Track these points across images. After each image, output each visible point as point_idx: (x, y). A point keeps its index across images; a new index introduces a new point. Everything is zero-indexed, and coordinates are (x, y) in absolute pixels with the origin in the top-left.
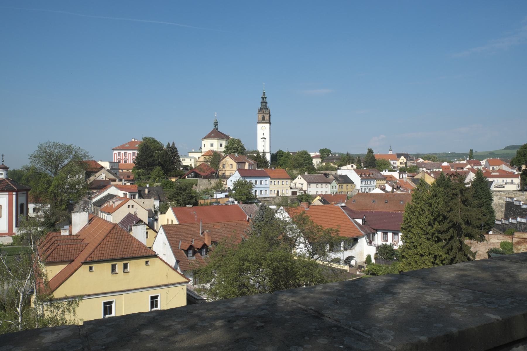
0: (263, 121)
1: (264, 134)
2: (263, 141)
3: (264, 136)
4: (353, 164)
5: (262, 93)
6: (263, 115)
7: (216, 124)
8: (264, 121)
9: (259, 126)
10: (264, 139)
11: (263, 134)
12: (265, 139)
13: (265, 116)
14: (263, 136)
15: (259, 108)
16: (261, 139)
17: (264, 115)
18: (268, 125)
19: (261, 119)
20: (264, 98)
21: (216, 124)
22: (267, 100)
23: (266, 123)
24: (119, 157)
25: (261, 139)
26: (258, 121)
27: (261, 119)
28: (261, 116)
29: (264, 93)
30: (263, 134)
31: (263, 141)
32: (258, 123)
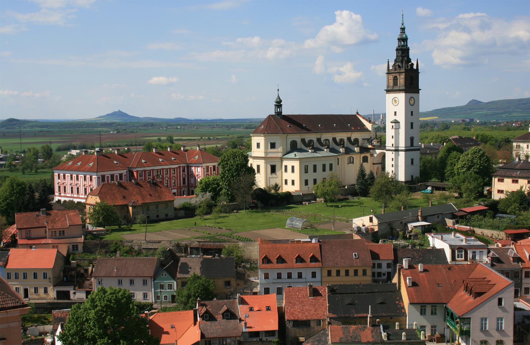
2: (393, 126)
3: (397, 118)
4: (371, 216)
5: (399, 31)
6: (394, 75)
7: (279, 104)
9: (390, 96)
10: (393, 124)
13: (398, 76)
15: (392, 64)
16: (392, 122)
17: (397, 75)
18: (401, 97)
19: (391, 82)
20: (403, 40)
21: (279, 104)
22: (409, 45)
23: (399, 91)
24: (59, 181)
26: (388, 86)
27: (391, 84)
28: (391, 77)
29: (403, 29)
31: (393, 126)
32: (388, 91)
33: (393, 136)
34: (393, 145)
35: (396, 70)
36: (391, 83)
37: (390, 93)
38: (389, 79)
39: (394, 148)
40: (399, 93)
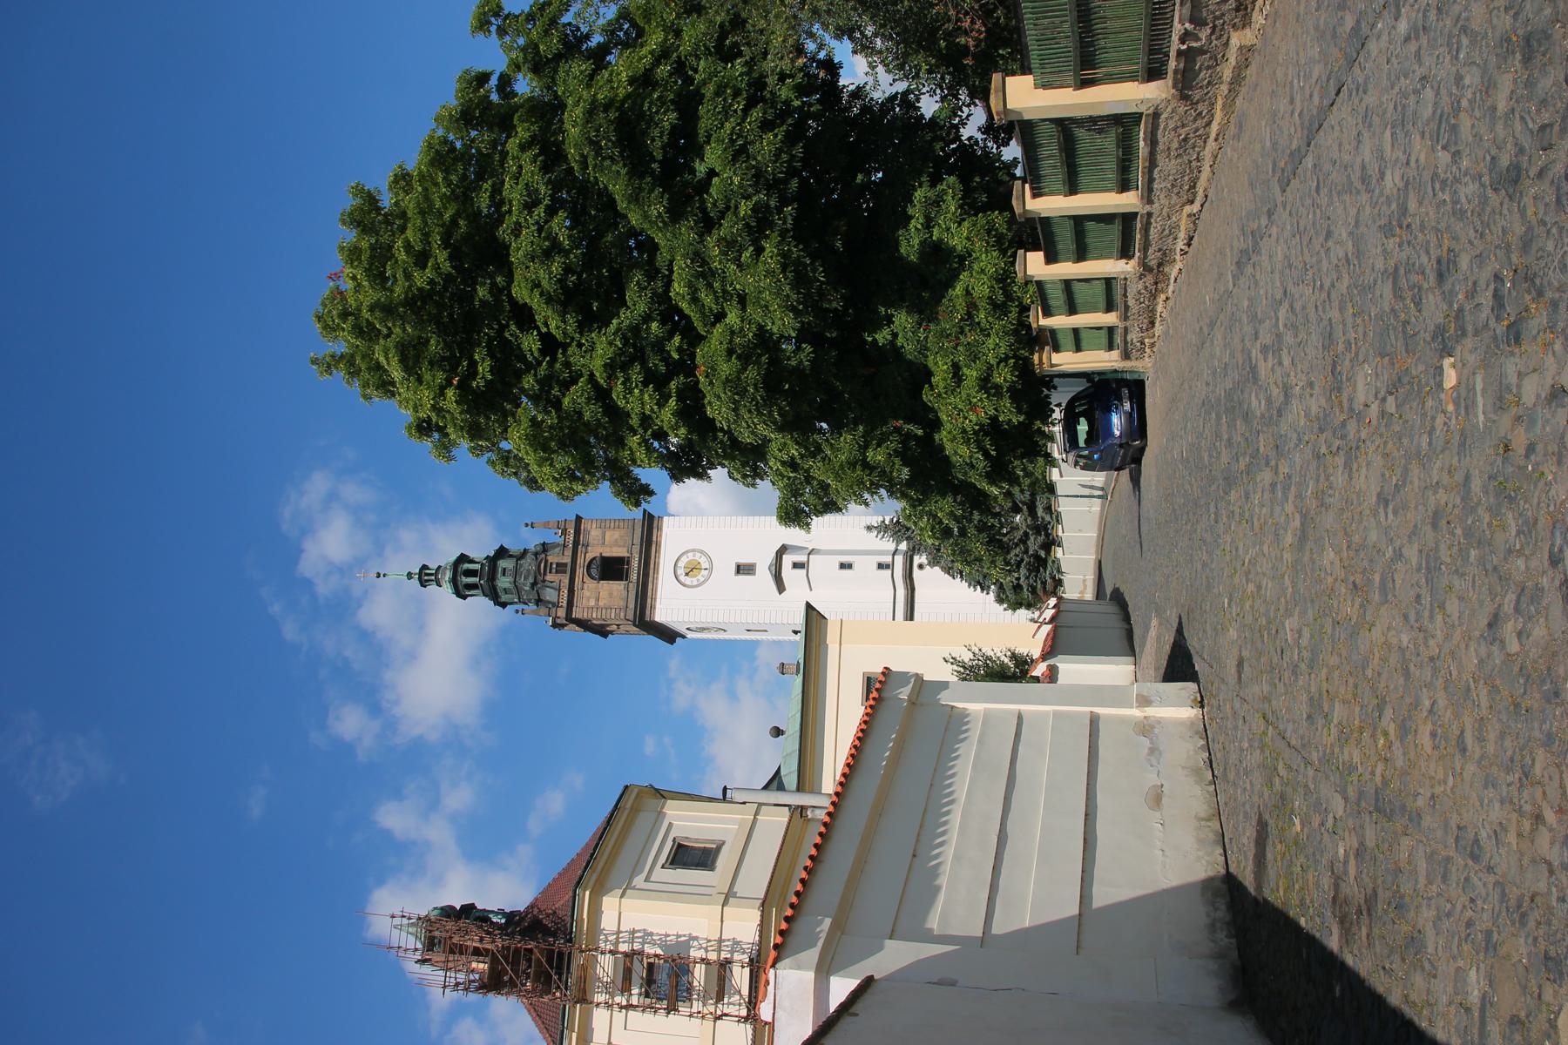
0: (634, 577)
1: (743, 560)
2: (796, 565)
3: (764, 562)
6: (580, 571)
8: (635, 564)
10: (788, 560)
11: (742, 569)
12: (783, 550)
14: (764, 575)
16: (781, 587)
17: (580, 560)
25: (781, 587)
27: (616, 587)
30: (742, 569)
31: (796, 565)
33: (843, 566)
34: (881, 566)
35: (565, 565)
36: (611, 595)
37: (654, 599)
38: (592, 603)
39: (899, 560)
40: (658, 545)
